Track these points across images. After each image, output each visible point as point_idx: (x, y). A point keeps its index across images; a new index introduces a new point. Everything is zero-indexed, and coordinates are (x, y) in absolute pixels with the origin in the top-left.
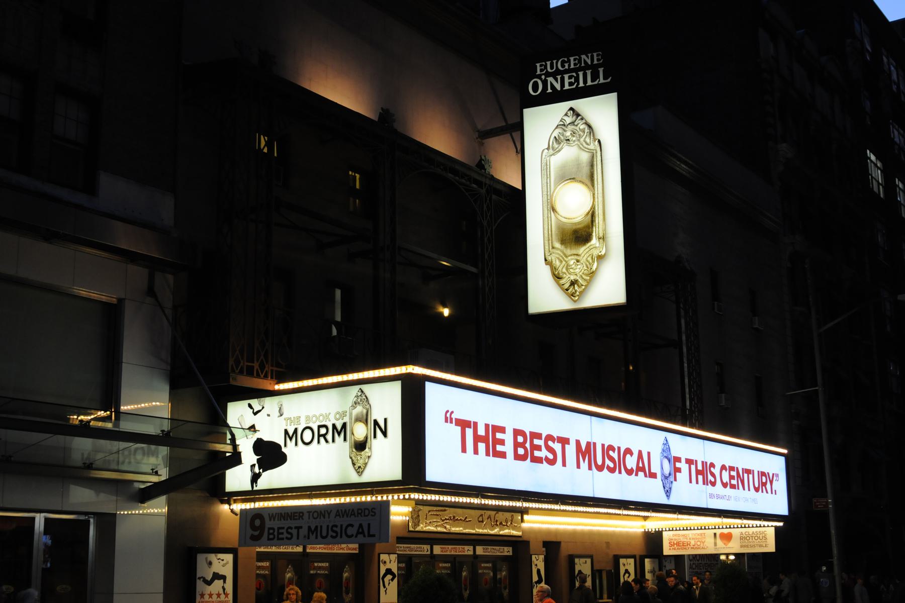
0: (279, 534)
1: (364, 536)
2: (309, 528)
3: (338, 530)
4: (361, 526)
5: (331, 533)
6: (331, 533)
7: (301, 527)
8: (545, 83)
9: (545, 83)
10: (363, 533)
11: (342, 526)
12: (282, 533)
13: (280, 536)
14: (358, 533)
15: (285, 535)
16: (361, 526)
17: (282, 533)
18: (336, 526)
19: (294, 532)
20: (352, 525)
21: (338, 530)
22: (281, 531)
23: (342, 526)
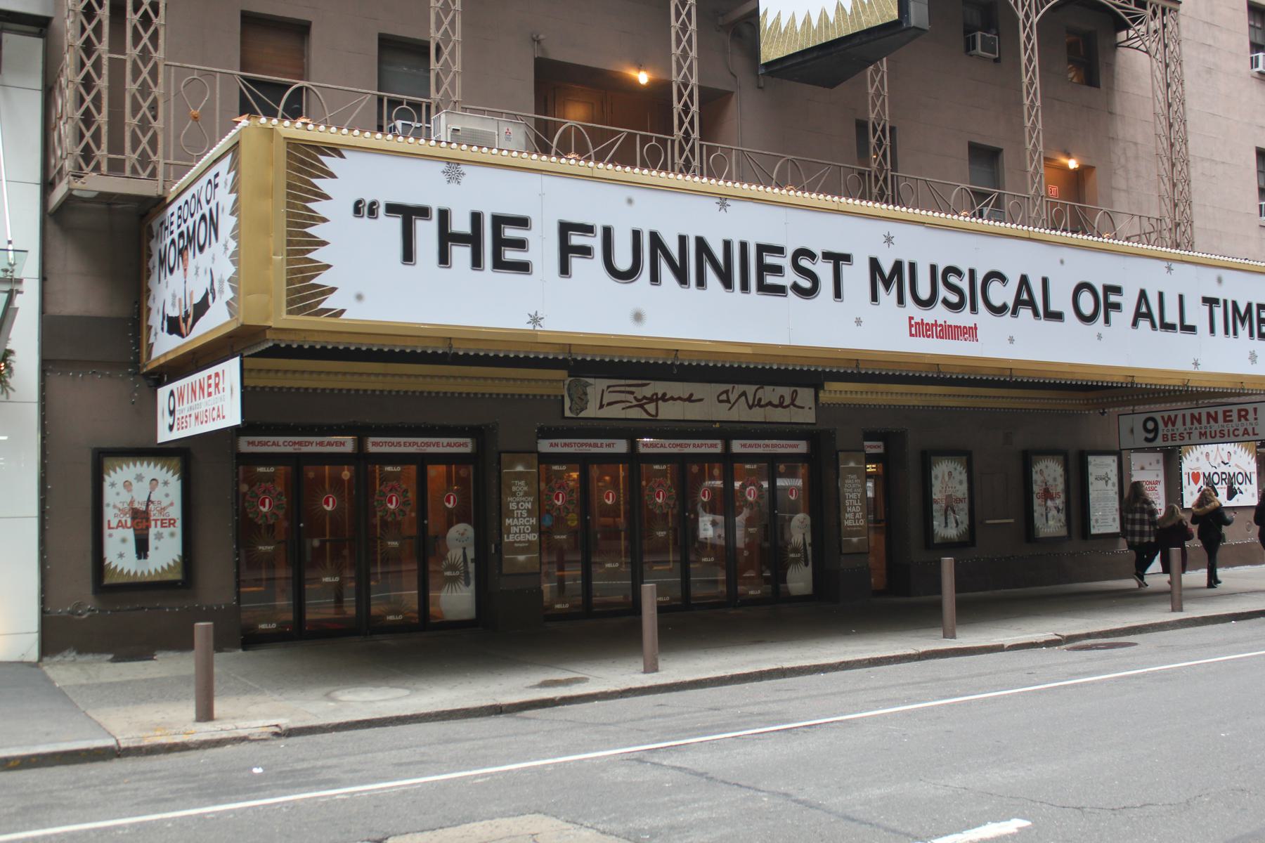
0: (763, 268)
1: (1036, 314)
2: (875, 265)
3: (964, 285)
4: (1024, 281)
5: (943, 292)
6: (943, 292)
7: (847, 258)
10: (1031, 303)
11: (972, 272)
12: (777, 270)
13: (770, 279)
14: (1019, 302)
15: (789, 277)
16: (1024, 281)
17: (777, 270)
18: (959, 273)
19: (824, 270)
21: (964, 285)
22: (770, 259)
23: (972, 272)
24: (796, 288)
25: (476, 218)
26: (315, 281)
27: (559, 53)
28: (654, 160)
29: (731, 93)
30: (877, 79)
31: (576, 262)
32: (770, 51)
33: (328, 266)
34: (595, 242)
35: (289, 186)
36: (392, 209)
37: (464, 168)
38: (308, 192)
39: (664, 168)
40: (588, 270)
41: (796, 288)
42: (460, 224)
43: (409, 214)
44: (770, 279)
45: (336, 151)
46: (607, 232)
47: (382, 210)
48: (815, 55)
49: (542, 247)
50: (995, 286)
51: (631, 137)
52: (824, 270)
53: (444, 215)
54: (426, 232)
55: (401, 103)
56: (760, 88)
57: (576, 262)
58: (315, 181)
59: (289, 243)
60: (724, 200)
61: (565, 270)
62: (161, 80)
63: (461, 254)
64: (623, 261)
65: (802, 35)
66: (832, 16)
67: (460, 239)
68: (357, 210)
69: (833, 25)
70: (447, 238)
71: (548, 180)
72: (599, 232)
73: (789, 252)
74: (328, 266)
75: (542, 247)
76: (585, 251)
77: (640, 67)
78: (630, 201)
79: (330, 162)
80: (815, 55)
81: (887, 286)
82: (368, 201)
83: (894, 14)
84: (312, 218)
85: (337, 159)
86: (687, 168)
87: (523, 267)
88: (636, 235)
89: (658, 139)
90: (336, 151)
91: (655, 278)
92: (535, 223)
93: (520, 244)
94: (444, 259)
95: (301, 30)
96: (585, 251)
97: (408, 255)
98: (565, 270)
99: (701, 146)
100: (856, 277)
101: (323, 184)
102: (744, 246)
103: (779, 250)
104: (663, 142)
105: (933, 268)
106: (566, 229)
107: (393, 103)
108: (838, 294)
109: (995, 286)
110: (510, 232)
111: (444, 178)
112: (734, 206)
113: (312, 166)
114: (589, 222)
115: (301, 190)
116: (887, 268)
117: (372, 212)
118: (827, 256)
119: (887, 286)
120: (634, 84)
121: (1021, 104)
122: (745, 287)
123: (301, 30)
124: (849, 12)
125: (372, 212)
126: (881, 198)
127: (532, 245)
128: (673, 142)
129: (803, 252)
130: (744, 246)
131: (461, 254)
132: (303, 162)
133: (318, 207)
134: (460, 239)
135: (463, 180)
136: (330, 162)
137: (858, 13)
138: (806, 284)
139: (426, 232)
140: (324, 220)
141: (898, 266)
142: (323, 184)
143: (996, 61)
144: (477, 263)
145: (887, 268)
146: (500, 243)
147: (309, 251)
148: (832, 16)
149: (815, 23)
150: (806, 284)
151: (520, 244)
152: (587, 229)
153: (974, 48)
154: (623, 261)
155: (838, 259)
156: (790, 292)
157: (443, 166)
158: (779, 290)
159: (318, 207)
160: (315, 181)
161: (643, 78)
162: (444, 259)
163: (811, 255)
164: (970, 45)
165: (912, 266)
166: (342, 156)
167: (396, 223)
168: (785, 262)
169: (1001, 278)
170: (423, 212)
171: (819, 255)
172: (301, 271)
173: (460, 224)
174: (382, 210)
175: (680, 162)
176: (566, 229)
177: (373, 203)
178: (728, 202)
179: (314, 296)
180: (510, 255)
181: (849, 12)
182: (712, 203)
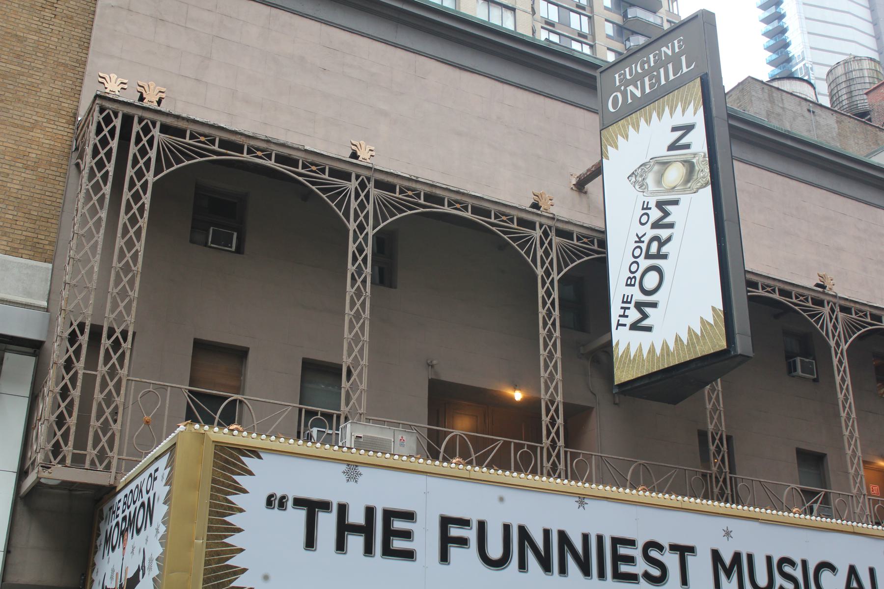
0: (618, 559)
3: (798, 574)
4: (852, 570)
7: (691, 550)
8: (624, 94)
9: (624, 94)
11: (804, 563)
12: (630, 560)
13: (624, 568)
15: (641, 567)
16: (852, 570)
17: (630, 560)
18: (792, 563)
19: (671, 561)
20: (832, 568)
21: (798, 574)
22: (623, 551)
24: (647, 576)
25: (370, 512)
26: (228, 563)
27: (449, 375)
28: (526, 465)
29: (592, 408)
30: (713, 396)
31: (454, 551)
32: (622, 375)
33: (242, 550)
34: (471, 534)
35: (214, 481)
36: (299, 502)
37: (361, 469)
38: (229, 486)
39: (534, 472)
40: (465, 558)
41: (647, 576)
42: (356, 517)
43: (313, 508)
44: (624, 568)
45: (255, 453)
46: (482, 525)
47: (290, 503)
48: (659, 377)
49: (425, 538)
50: (826, 575)
51: (506, 445)
52: (671, 561)
53: (343, 509)
54: (327, 523)
55: (316, 413)
56: (615, 404)
57: (454, 551)
58: (236, 477)
59: (210, 529)
60: (582, 499)
61: (444, 557)
62: (123, 392)
63: (355, 542)
64: (495, 550)
65: (648, 362)
66: (672, 346)
67: (355, 529)
68: (269, 502)
69: (673, 354)
70: (344, 528)
71: (432, 480)
72: (475, 525)
73: (640, 545)
74: (242, 550)
75: (425, 538)
76: (462, 542)
77: (516, 387)
78: (501, 499)
79: (250, 462)
80: (659, 377)
81: (729, 575)
82: (279, 496)
83: (723, 344)
84: (231, 509)
85: (256, 459)
86: (553, 471)
87: (408, 555)
88: (507, 528)
89: (529, 447)
90: (255, 453)
91: (523, 566)
92: (419, 517)
93: (407, 535)
94: (341, 546)
95: (240, 354)
96: (462, 542)
97: (310, 542)
98: (444, 557)
99: (566, 452)
100: (700, 567)
101: (242, 480)
102: (600, 539)
103: (631, 543)
104: (534, 449)
105: (769, 559)
106: (446, 522)
107: (310, 414)
108: (684, 581)
109: (826, 575)
110: (398, 525)
111: (344, 477)
112: (591, 504)
113: (235, 465)
114: (466, 516)
115: (223, 484)
116: (727, 559)
117: (282, 505)
118: (674, 548)
119: (729, 575)
120: (512, 399)
121: (838, 415)
122: (602, 575)
123: (240, 354)
124: (685, 343)
125: (282, 505)
126: (721, 497)
127: (416, 536)
128: (542, 448)
129: (652, 545)
130: (600, 539)
131: (355, 542)
132: (227, 461)
133: (237, 499)
134: (355, 529)
135: (360, 479)
136: (250, 462)
137: (693, 344)
138: (656, 572)
139: (327, 523)
140: (241, 510)
141: (737, 557)
142: (242, 480)
143: (815, 380)
144: (369, 550)
145: (727, 559)
146: (389, 533)
147: (226, 537)
148: (672, 346)
149: (658, 351)
150: (656, 572)
151: (407, 535)
152: (464, 523)
153: (795, 370)
154: (495, 550)
155: (683, 551)
156: (642, 580)
157: (344, 467)
158: (632, 578)
159: (237, 499)
160: (236, 477)
161: (518, 396)
162: (341, 546)
163: (660, 548)
164: (791, 368)
165: (750, 557)
166: (260, 457)
167: (301, 515)
168: (636, 553)
169: (832, 568)
170: (325, 506)
171: (667, 547)
172: (218, 553)
173: (356, 517)
174: (290, 503)
175: (548, 465)
176: (446, 522)
177: (283, 497)
178: (586, 501)
179: (227, 575)
180: (398, 544)
181: (685, 343)
182: (572, 502)
